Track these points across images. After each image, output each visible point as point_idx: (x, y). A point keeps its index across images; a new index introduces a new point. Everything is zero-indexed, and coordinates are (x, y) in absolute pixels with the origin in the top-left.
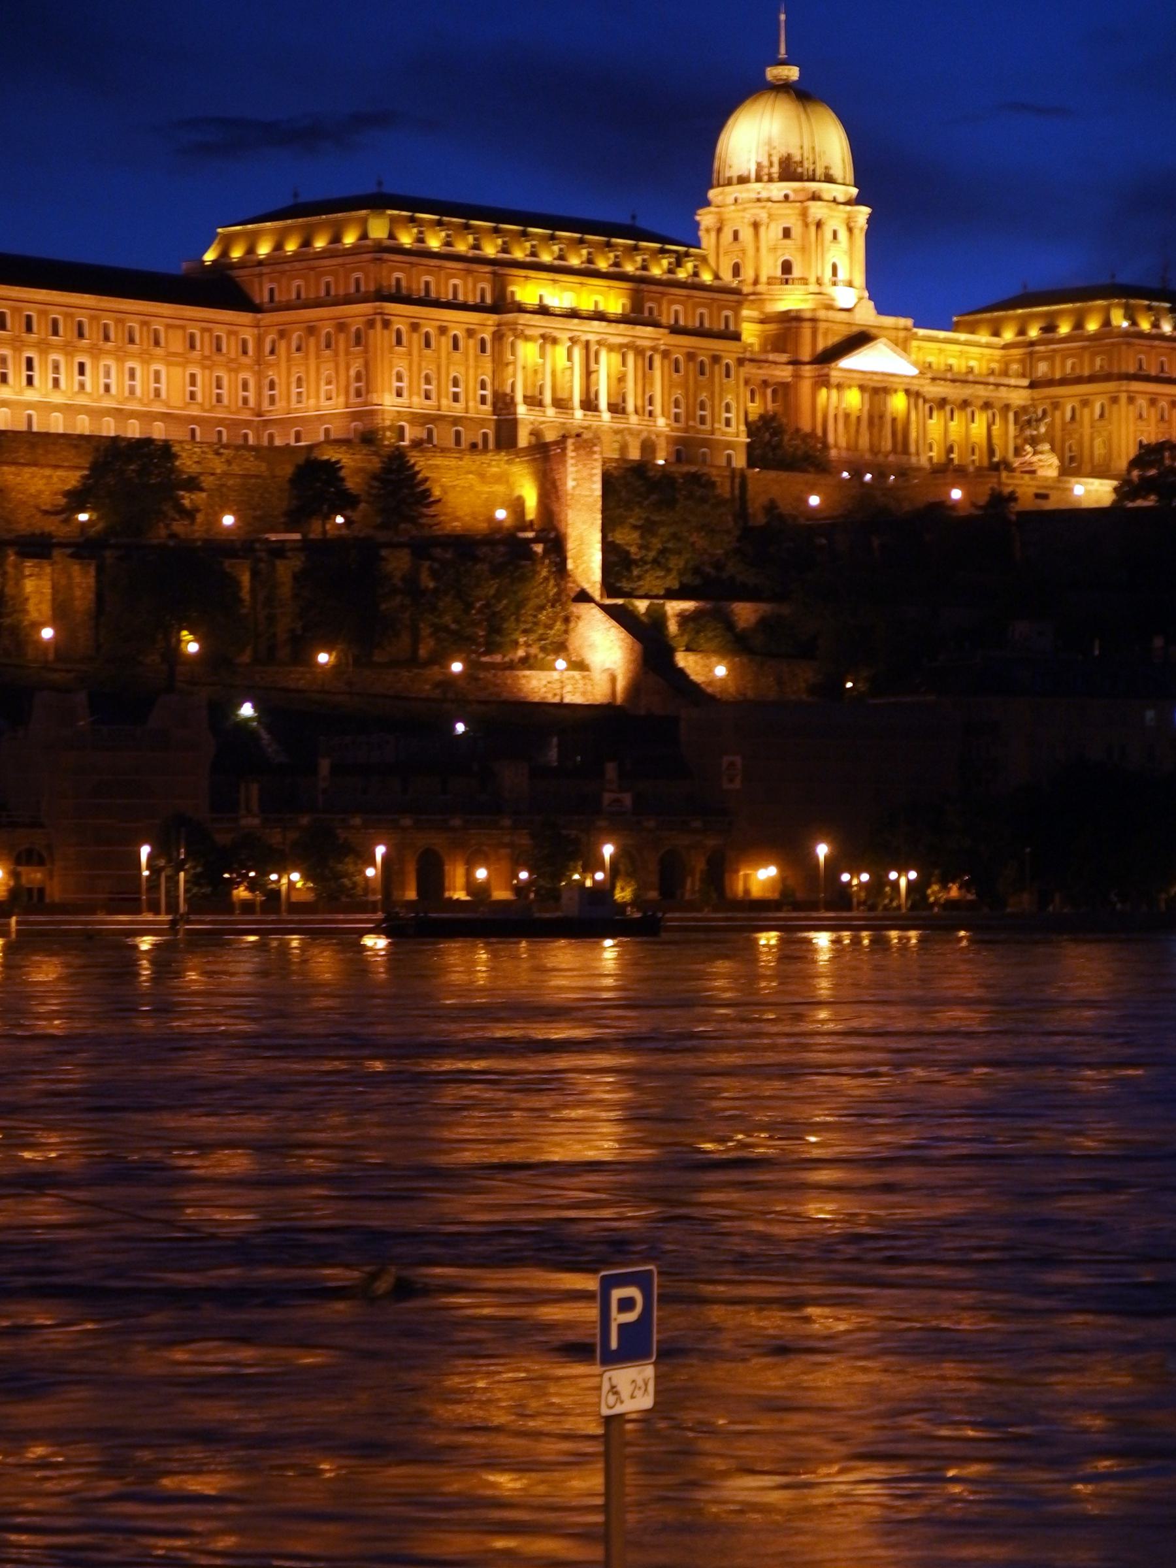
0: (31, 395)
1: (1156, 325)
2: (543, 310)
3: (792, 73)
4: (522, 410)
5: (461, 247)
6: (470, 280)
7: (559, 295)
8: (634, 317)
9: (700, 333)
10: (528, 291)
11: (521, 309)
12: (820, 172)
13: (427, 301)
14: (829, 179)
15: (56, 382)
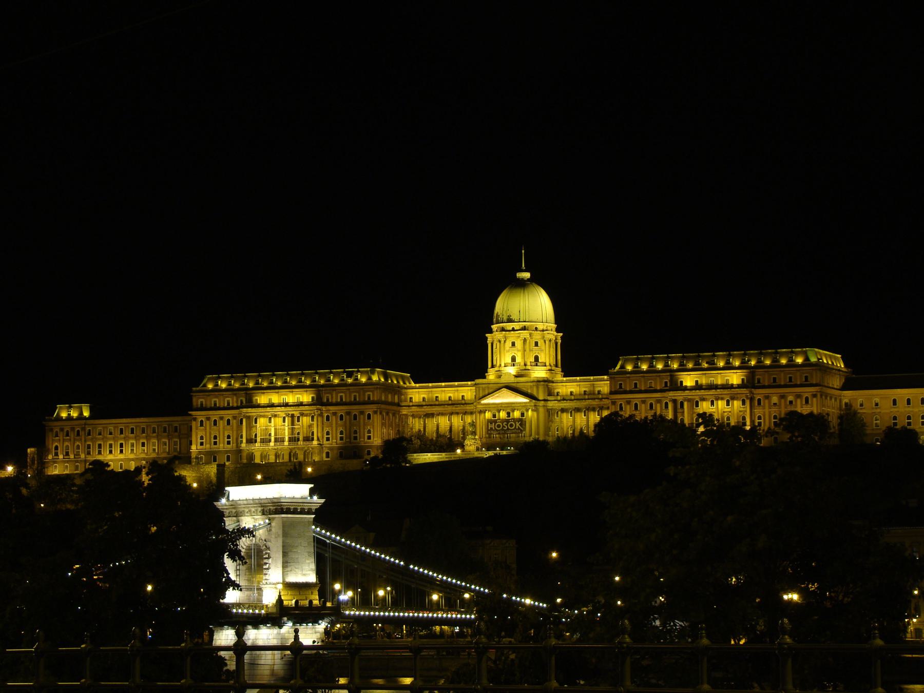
0: (122, 456)
1: (636, 366)
2: (272, 405)
3: (527, 275)
4: (244, 445)
5: (237, 385)
6: (221, 397)
7: (275, 398)
8: (318, 401)
9: (355, 403)
10: (262, 399)
11: (259, 406)
12: (505, 319)
13: (216, 408)
14: (510, 320)
15: (132, 450)
